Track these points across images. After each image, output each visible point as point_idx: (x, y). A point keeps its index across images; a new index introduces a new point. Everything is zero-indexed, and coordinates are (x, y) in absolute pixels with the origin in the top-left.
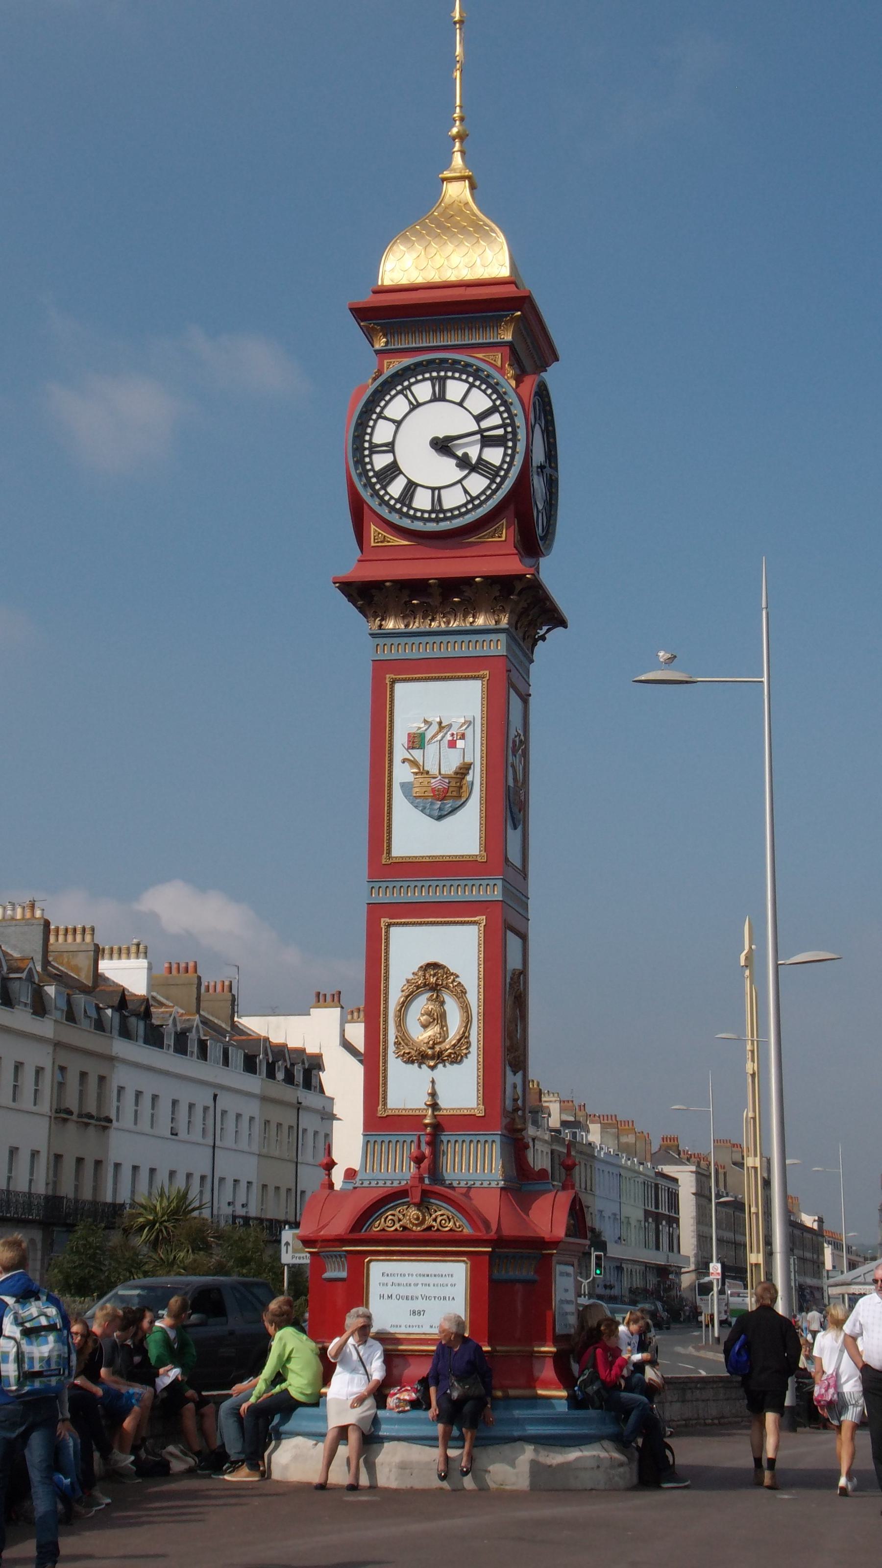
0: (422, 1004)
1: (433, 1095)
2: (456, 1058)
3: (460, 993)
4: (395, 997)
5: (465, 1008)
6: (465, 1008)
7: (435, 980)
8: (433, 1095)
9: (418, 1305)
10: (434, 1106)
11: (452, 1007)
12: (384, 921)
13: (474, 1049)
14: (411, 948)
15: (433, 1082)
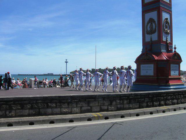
0: (149, 25)
1: (151, 38)
2: (154, 32)
3: (154, 22)
4: (146, 24)
5: (155, 24)
6: (155, 24)
7: (151, 20)
8: (151, 38)
9: (147, 71)
10: (152, 40)
11: (154, 25)
12: (144, 13)
13: (157, 30)
14: (148, 16)
15: (151, 37)
